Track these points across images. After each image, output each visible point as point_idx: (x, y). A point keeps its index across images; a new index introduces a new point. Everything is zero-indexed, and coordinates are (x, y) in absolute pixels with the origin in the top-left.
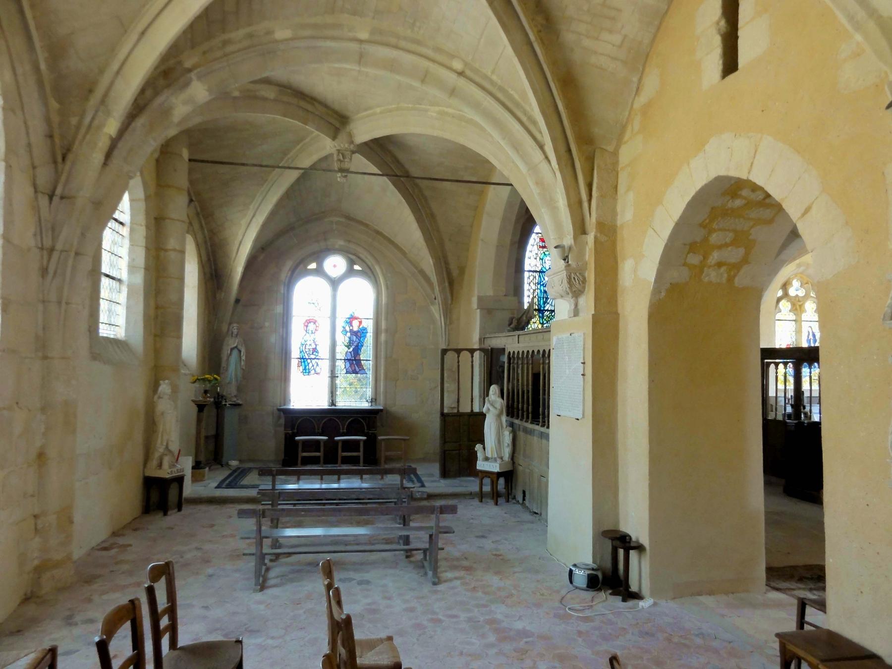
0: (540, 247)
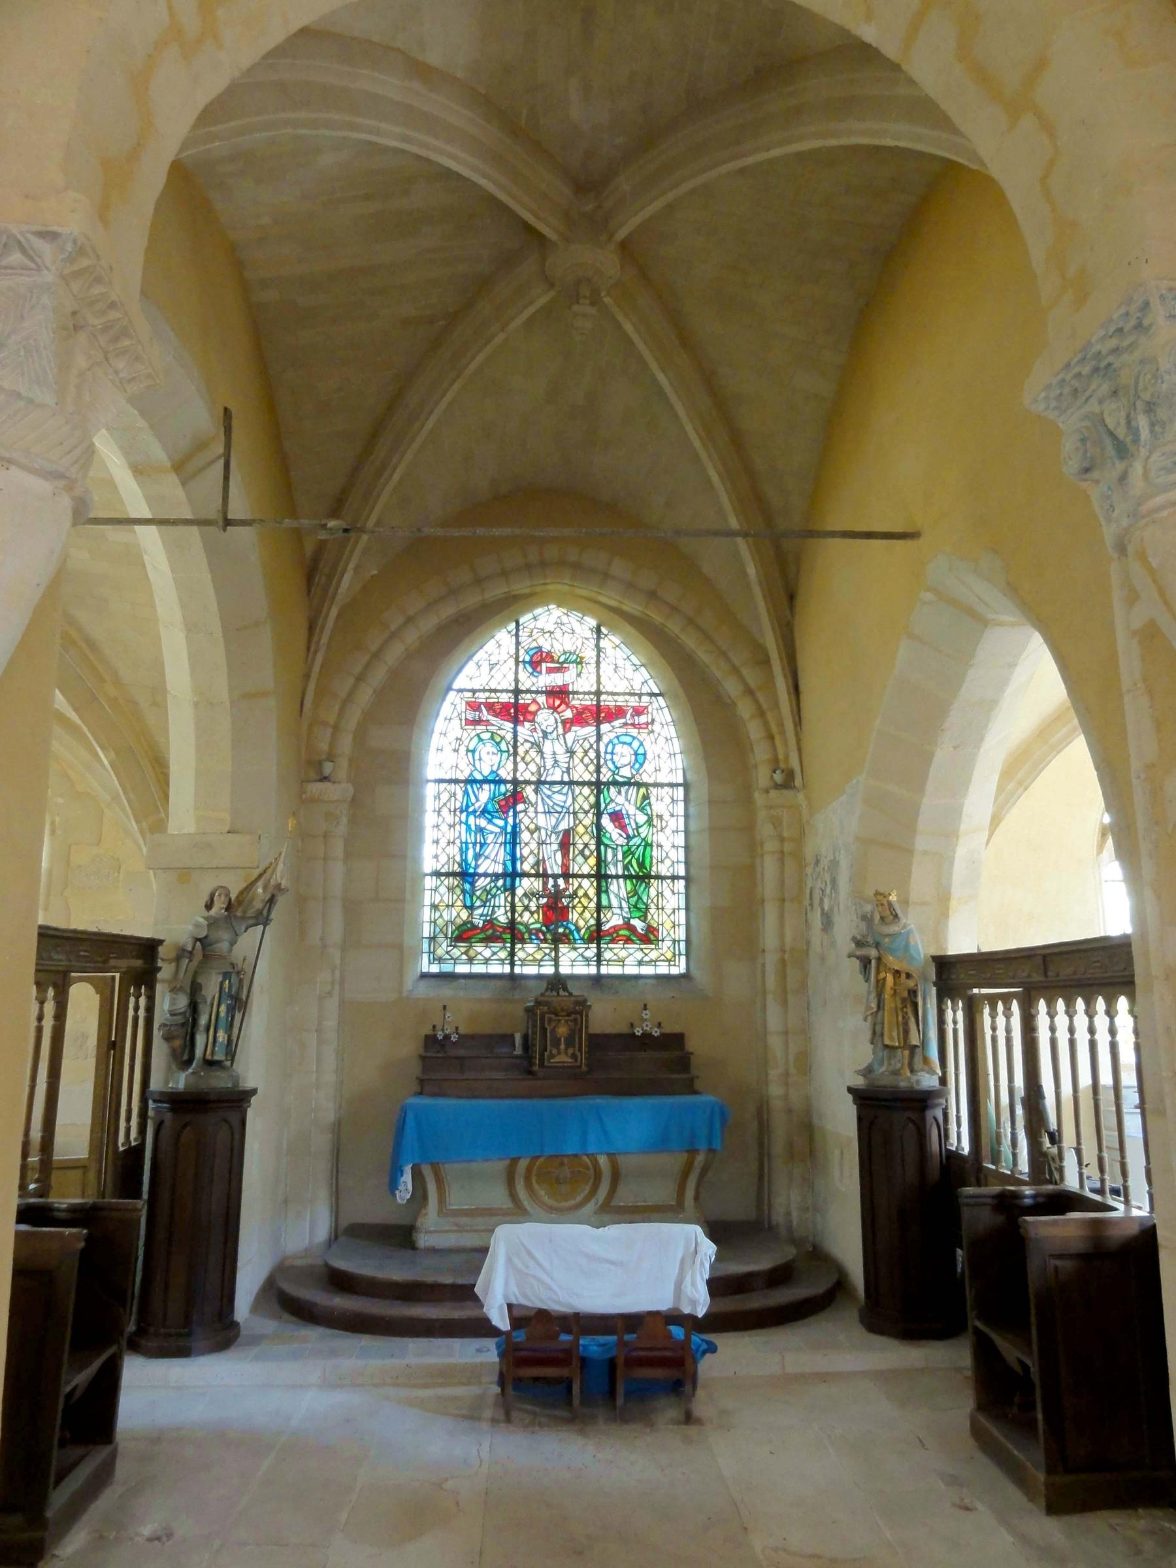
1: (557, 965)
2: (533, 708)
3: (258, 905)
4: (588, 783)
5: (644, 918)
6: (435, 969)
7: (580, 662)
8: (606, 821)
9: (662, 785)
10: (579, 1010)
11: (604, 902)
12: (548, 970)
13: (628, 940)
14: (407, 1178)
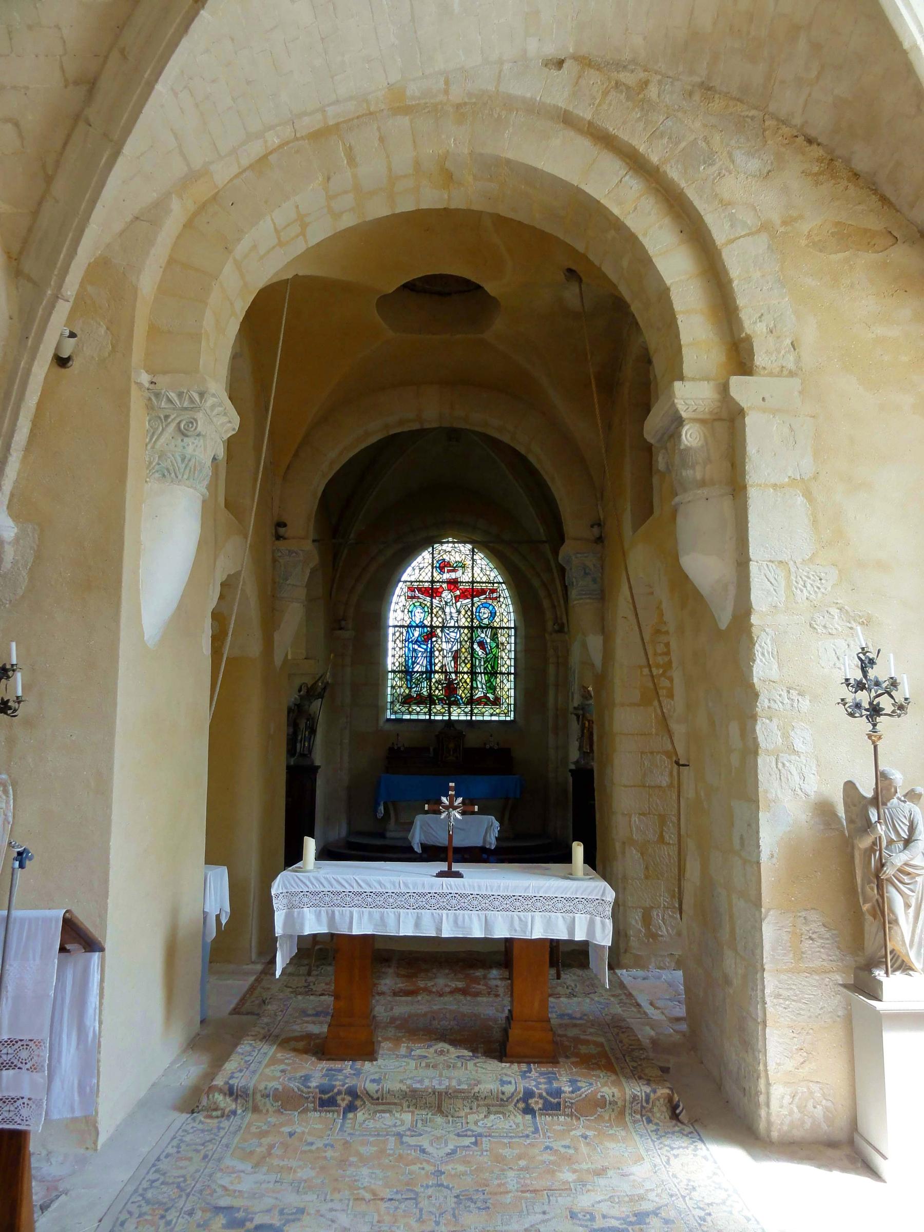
0: (409, 597)
1: (450, 716)
2: (440, 590)
3: (319, 690)
4: (467, 627)
5: (494, 693)
6: (393, 717)
7: (463, 566)
8: (476, 646)
9: (504, 628)
10: (460, 736)
11: (475, 685)
12: (446, 718)
13: (486, 704)
14: (382, 808)
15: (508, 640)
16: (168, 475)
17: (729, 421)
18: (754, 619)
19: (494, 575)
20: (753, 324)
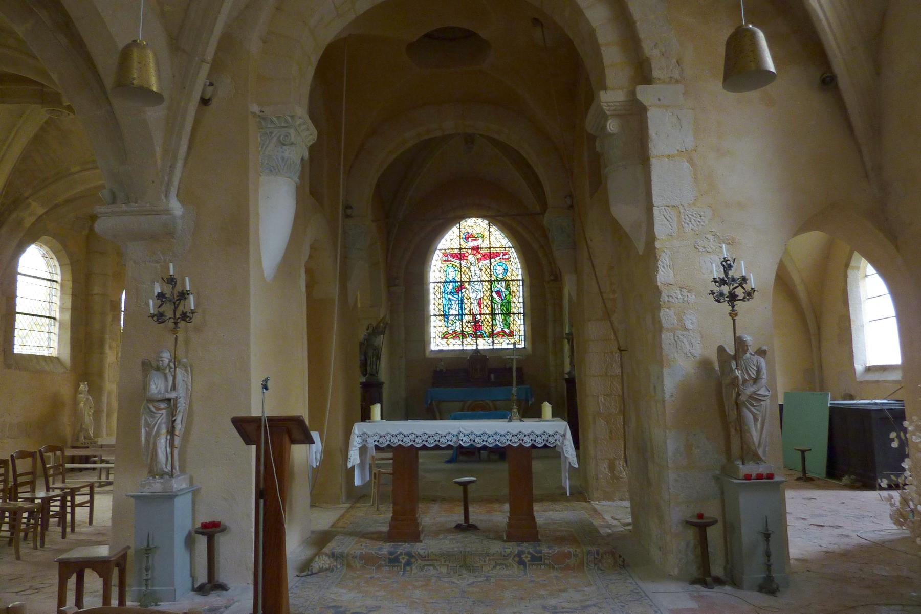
5: (508, 328)
7: (483, 237)
8: (494, 294)
12: (474, 348)
13: (503, 336)
15: (518, 290)
16: (273, 170)
17: (636, 114)
18: (657, 244)
19: (506, 242)
20: (649, 49)
